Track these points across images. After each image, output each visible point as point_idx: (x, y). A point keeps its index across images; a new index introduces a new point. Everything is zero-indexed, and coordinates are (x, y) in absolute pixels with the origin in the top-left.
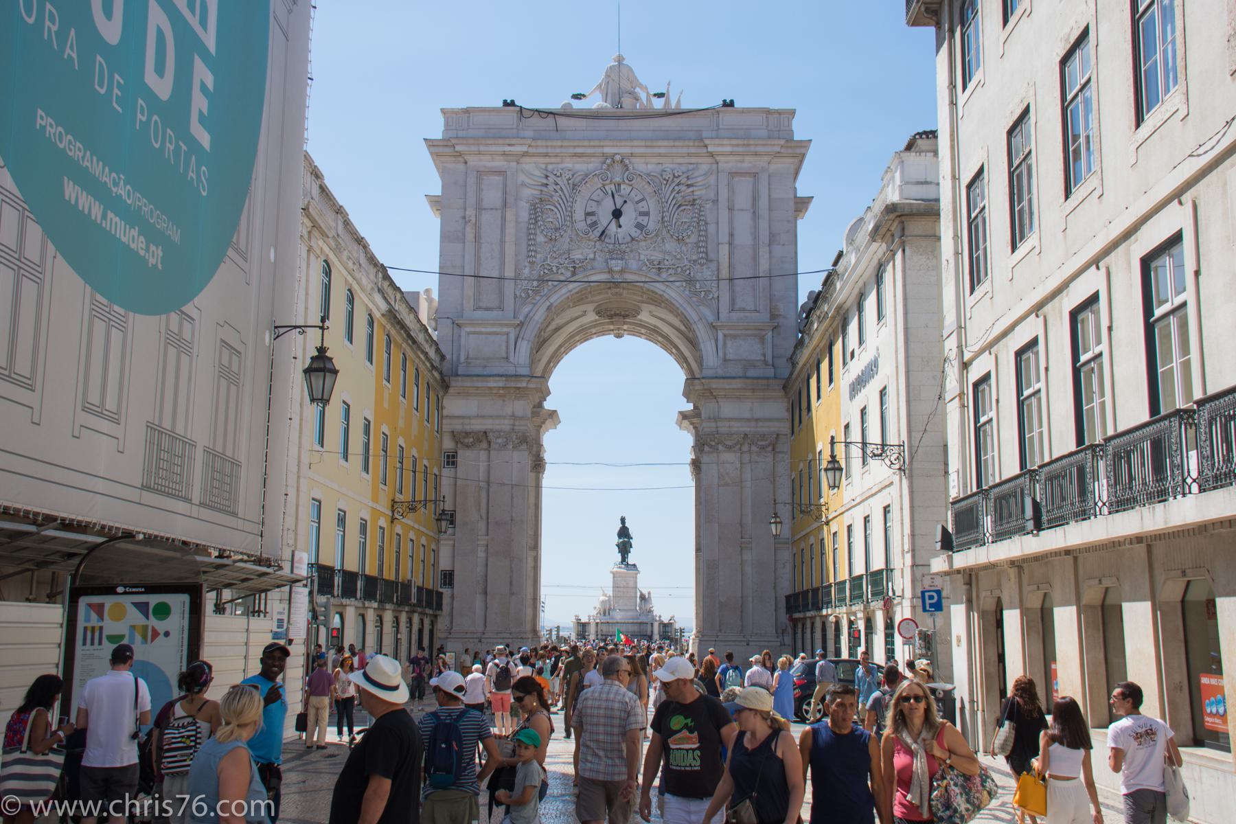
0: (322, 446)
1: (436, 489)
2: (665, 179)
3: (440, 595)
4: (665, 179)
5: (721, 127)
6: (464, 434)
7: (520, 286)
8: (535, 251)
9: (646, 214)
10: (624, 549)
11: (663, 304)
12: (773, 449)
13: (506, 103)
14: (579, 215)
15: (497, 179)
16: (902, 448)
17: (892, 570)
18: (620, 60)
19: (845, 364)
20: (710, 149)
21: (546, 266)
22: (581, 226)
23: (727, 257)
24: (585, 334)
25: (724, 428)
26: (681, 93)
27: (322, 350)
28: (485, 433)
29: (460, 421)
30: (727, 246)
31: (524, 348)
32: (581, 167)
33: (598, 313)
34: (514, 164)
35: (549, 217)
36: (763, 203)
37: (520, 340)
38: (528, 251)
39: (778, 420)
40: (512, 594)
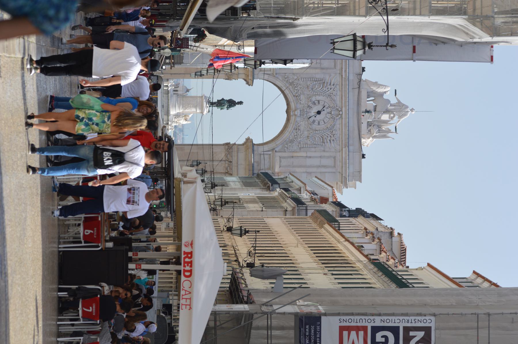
5: (355, 153)
9: (319, 124)
10: (220, 104)
12: (226, 172)
13: (364, 68)
14: (318, 98)
15: (333, 66)
20: (344, 149)
21: (297, 85)
22: (314, 99)
23: (302, 155)
25: (234, 154)
26: (393, 139)
30: (305, 155)
32: (338, 99)
34: (338, 72)
36: (323, 170)
37: (268, 75)
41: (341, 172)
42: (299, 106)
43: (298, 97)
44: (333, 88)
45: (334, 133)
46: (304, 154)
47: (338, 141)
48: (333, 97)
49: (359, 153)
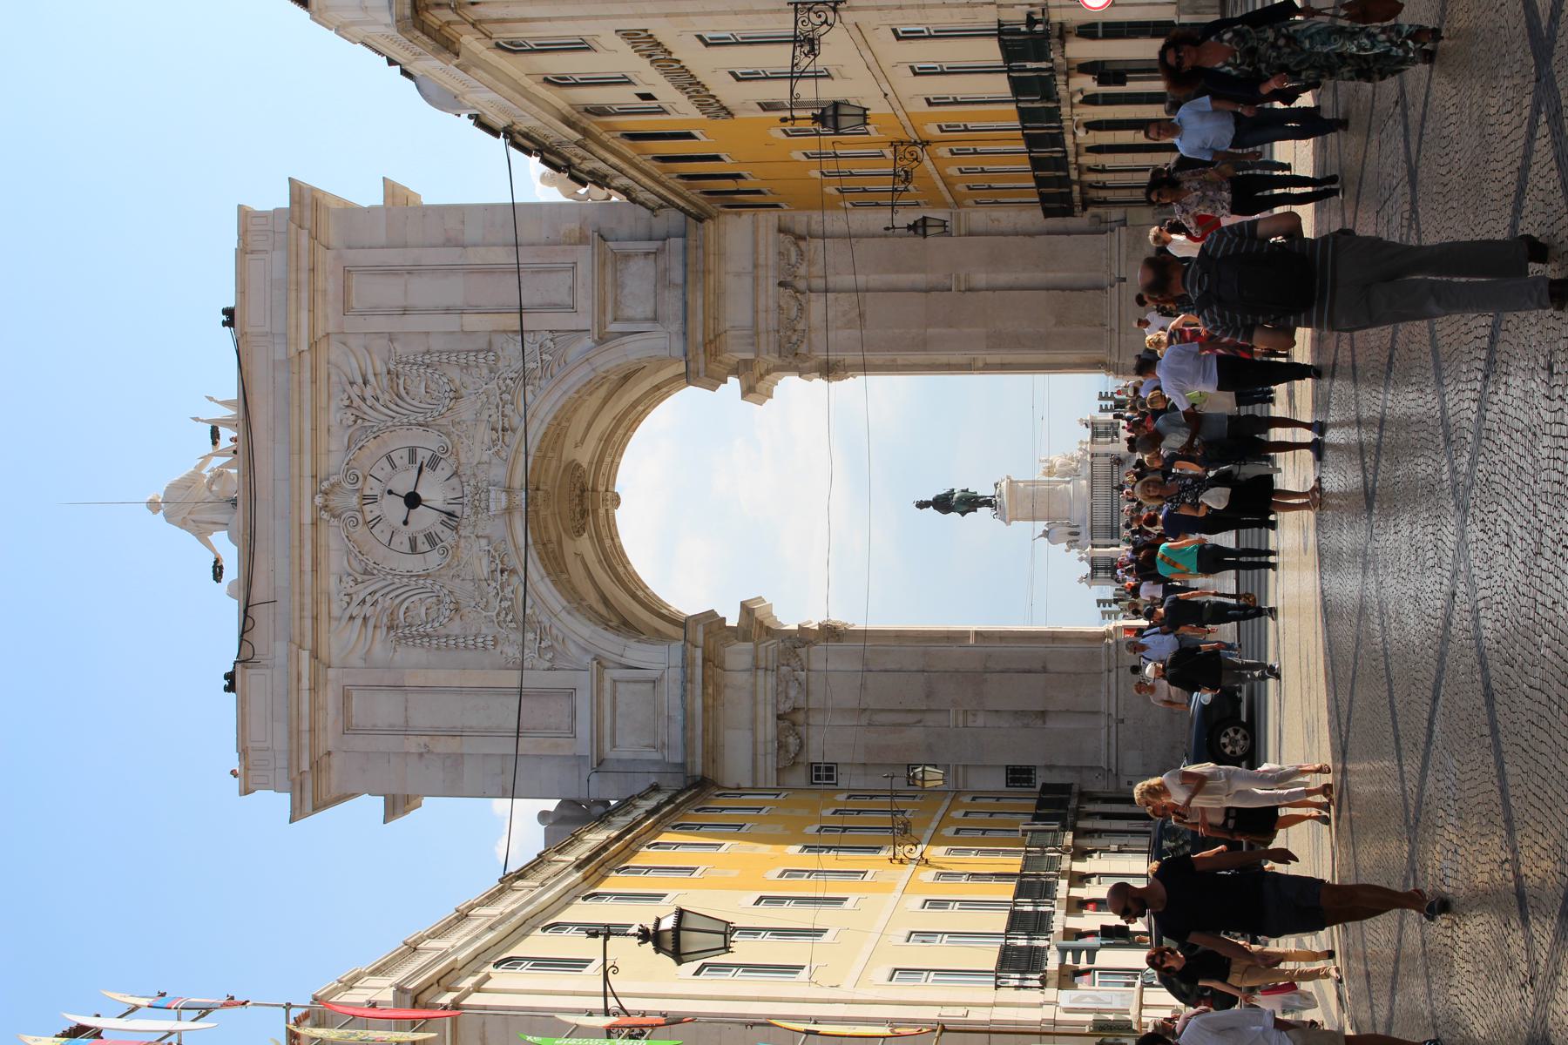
0: (802, 967)
1: (872, 797)
2: (355, 422)
3: (1046, 788)
4: (355, 422)
5: (267, 329)
6: (782, 752)
7: (535, 662)
8: (476, 637)
9: (413, 452)
10: (969, 503)
11: (564, 424)
12: (803, 238)
13: (230, 688)
14: (414, 564)
16: (799, 6)
17: (1000, 24)
18: (153, 506)
19: (664, 112)
20: (305, 347)
21: (501, 618)
22: (434, 559)
24: (613, 558)
25: (769, 321)
27: (644, 935)
28: (779, 717)
29: (760, 758)
31: (639, 653)
32: (335, 561)
33: (579, 532)
34: (331, 673)
35: (419, 615)
37: (623, 661)
38: (476, 648)
39: (755, 231)
40: (1045, 670)
41: (320, 251)
42: (496, 528)
43: (500, 566)
44: (354, 604)
45: (349, 412)
46: (473, 322)
47: (334, 378)
48: (355, 563)
49: (248, 329)
